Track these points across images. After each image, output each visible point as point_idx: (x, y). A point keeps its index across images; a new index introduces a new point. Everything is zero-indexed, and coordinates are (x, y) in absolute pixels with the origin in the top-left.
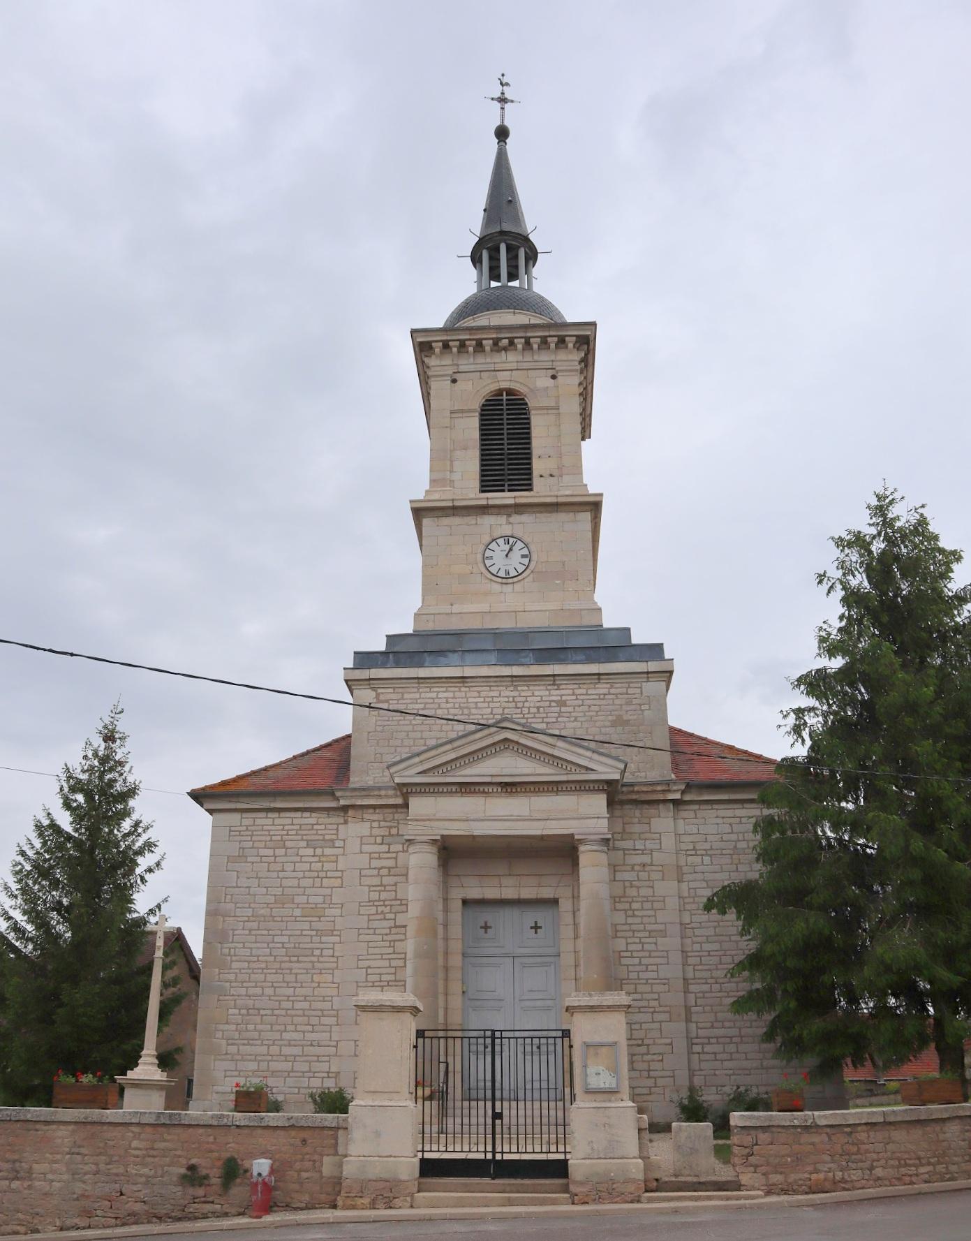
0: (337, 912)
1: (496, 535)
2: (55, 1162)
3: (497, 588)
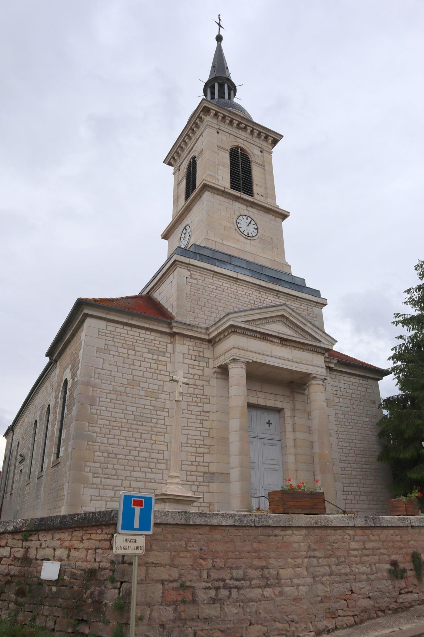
0: (167, 397)
1: (242, 213)
2: (298, 566)
3: (243, 239)
